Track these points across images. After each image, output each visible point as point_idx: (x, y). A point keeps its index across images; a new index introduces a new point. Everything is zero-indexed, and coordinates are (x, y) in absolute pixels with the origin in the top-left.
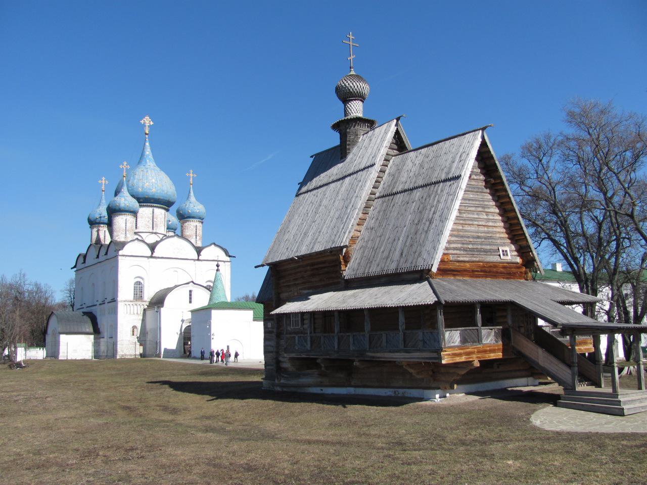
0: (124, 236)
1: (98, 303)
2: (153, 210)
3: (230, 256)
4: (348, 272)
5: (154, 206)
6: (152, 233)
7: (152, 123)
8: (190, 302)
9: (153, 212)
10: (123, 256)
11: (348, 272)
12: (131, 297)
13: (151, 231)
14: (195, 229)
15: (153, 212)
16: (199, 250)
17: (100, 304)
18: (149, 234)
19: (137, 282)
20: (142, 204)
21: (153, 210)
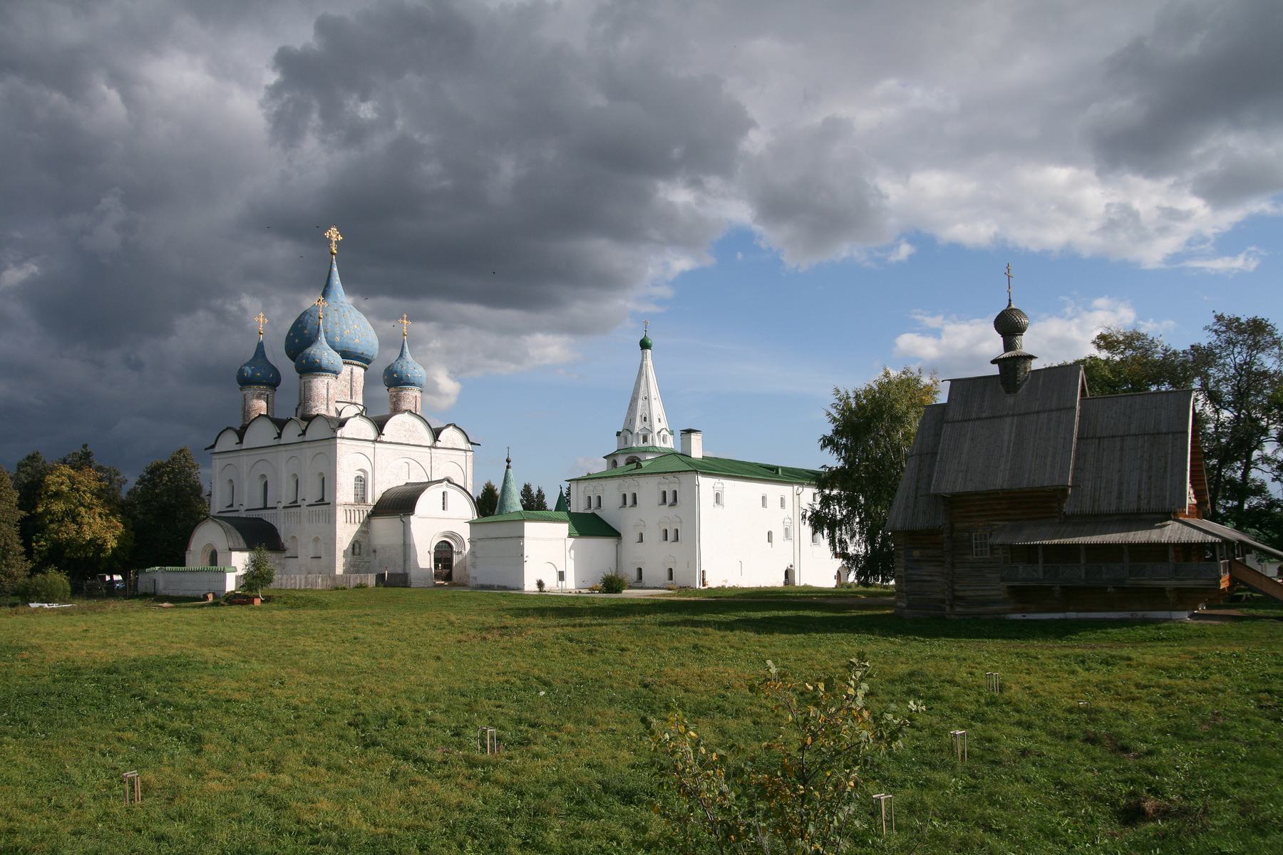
0: (325, 407)
1: (281, 506)
2: (352, 369)
3: (472, 444)
4: (1068, 508)
5: (353, 364)
6: (351, 403)
7: (340, 238)
8: (444, 509)
9: (352, 373)
10: (343, 438)
11: (1068, 508)
12: (352, 499)
13: (349, 400)
14: (414, 401)
15: (352, 373)
16: (436, 434)
17: (285, 507)
18: (347, 404)
19: (358, 477)
20: (347, 361)
21: (352, 369)
